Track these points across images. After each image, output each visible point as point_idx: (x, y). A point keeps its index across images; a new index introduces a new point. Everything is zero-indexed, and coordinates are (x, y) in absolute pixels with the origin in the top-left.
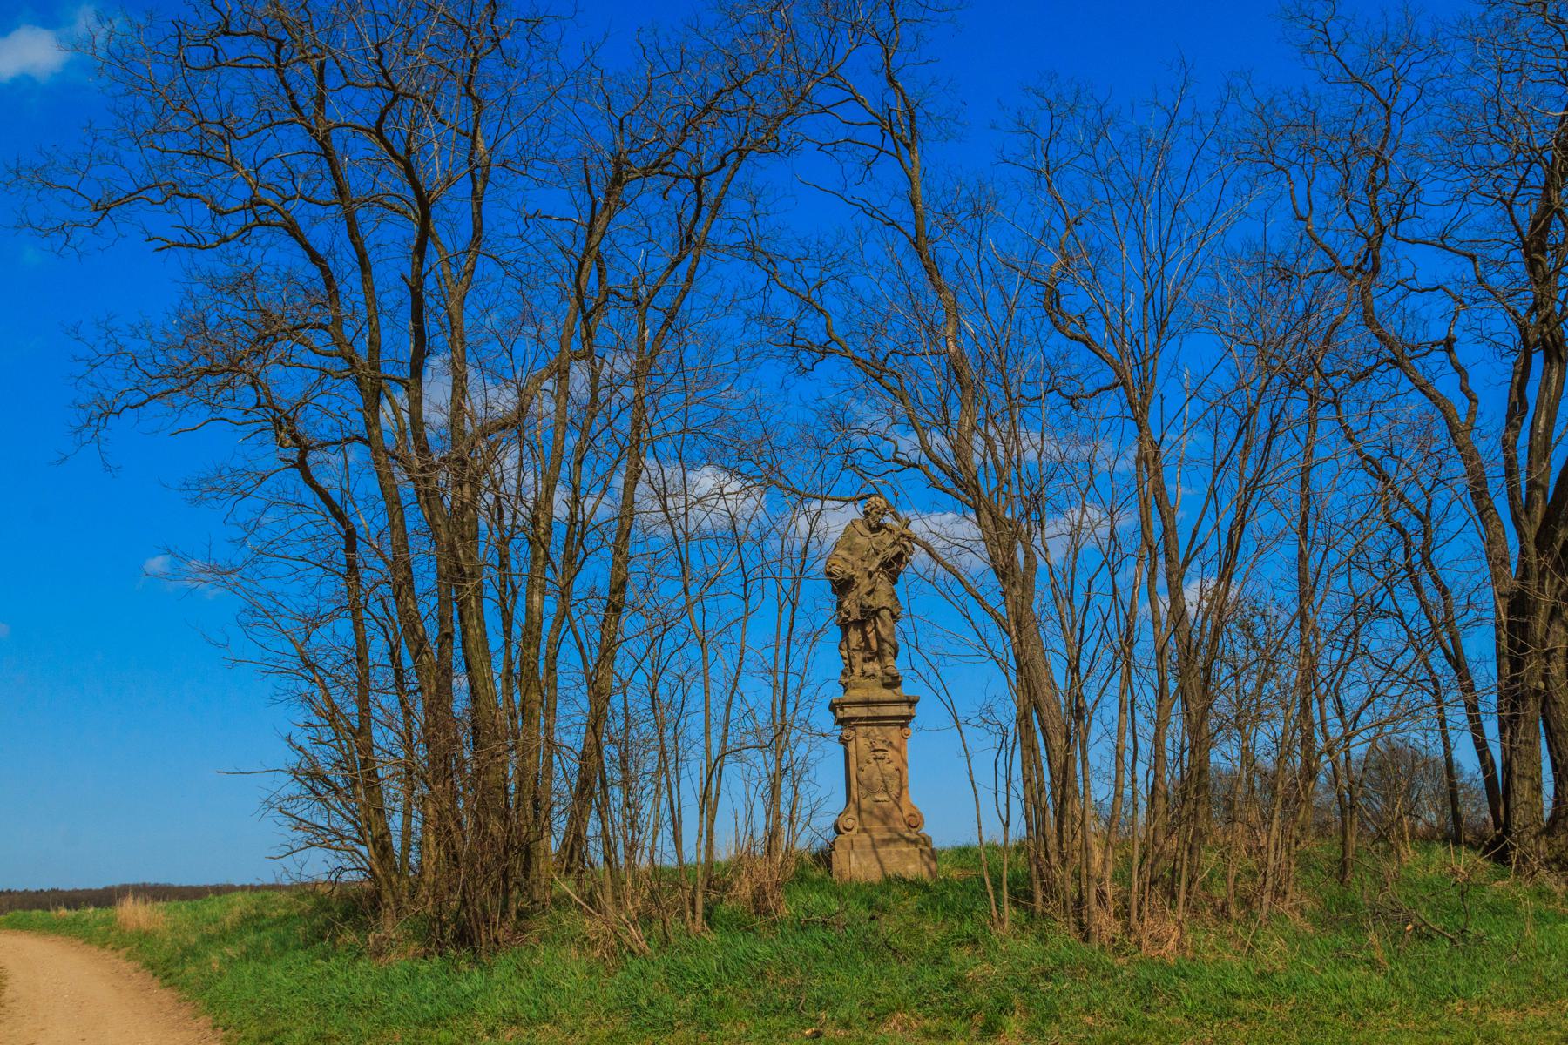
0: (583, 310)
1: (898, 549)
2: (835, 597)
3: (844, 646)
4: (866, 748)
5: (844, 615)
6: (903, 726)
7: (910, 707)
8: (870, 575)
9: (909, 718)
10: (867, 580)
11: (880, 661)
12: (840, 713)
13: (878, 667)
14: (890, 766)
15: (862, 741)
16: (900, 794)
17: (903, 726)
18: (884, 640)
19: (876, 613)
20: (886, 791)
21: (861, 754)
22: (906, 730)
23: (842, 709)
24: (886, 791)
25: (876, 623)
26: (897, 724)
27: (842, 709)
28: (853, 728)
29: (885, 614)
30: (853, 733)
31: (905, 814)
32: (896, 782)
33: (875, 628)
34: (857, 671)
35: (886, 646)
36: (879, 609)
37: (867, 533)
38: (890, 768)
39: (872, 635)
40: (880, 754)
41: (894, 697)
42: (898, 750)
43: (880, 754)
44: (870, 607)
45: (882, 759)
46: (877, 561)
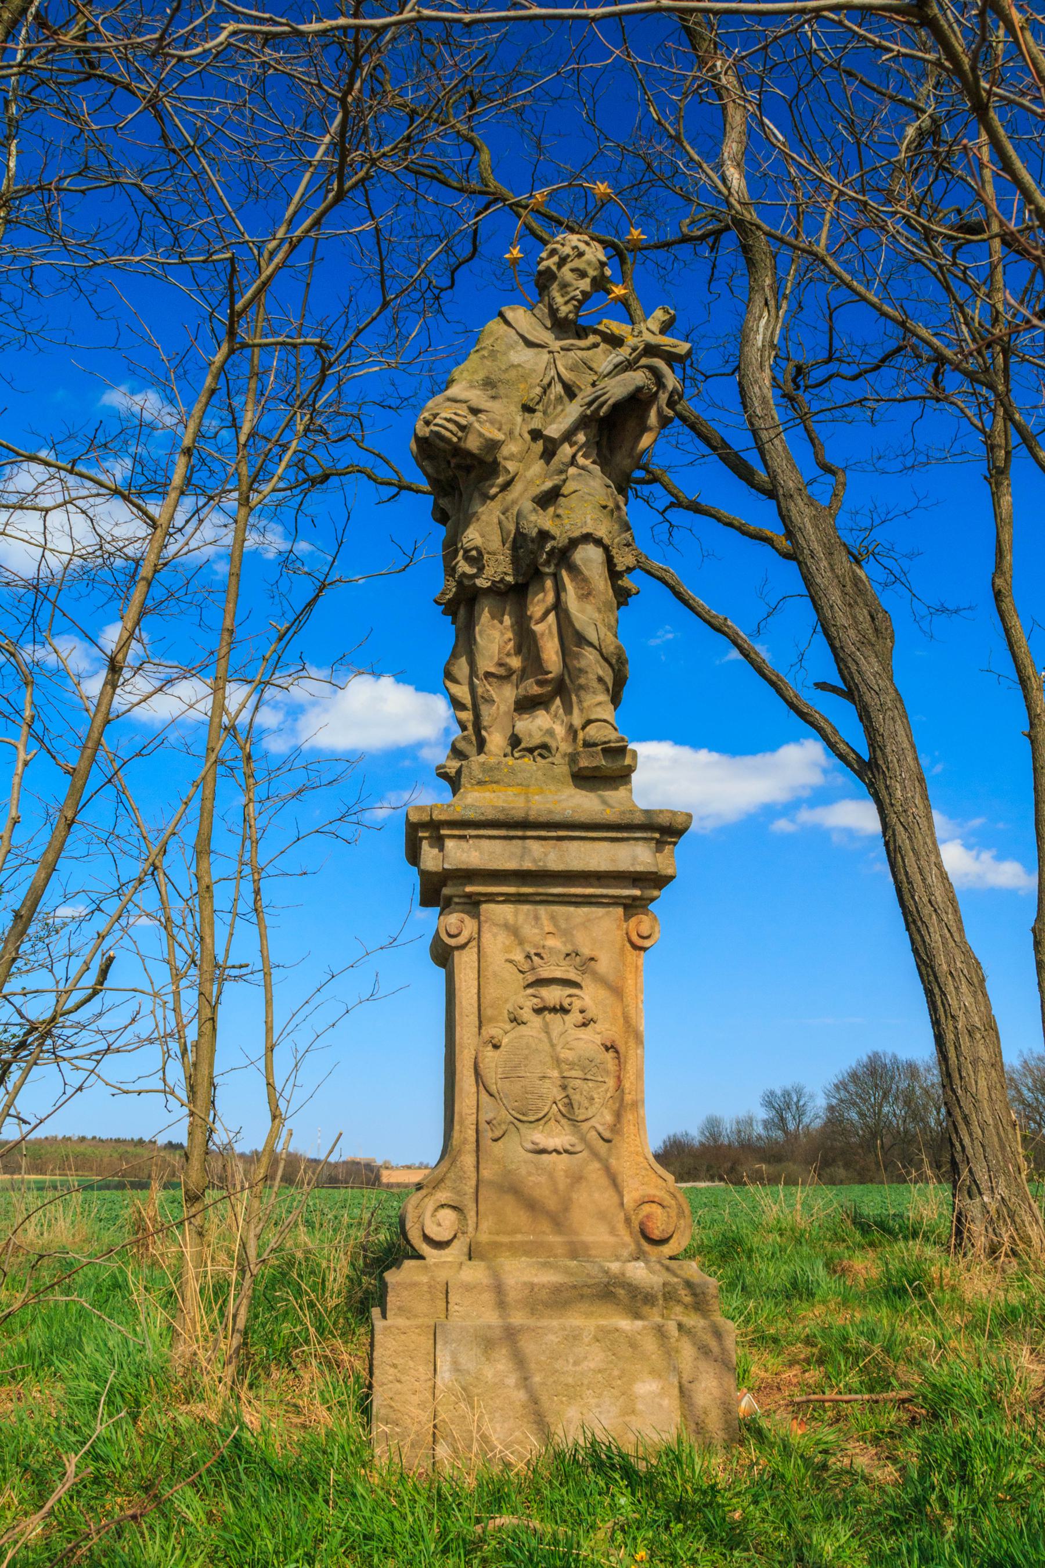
0: (30, 93)
1: (638, 378)
2: (441, 532)
3: (462, 668)
4: (509, 973)
5: (464, 567)
6: (632, 907)
7: (660, 845)
8: (549, 454)
9: (658, 880)
10: (537, 467)
11: (568, 709)
12: (431, 858)
13: (560, 730)
14: (585, 1034)
15: (495, 942)
16: (616, 1127)
17: (632, 907)
18: (581, 640)
19: (563, 556)
20: (570, 1114)
21: (492, 992)
22: (643, 923)
23: (439, 842)
24: (570, 1114)
25: (559, 588)
26: (615, 901)
27: (439, 842)
28: (473, 905)
29: (589, 557)
30: (470, 926)
31: (630, 1198)
32: (604, 1090)
33: (558, 607)
34: (496, 741)
35: (589, 658)
36: (574, 543)
37: (546, 337)
38: (588, 1041)
39: (546, 630)
40: (553, 995)
41: (610, 815)
42: (617, 992)
43: (553, 995)
44: (544, 535)
45: (564, 1010)
46: (573, 411)
